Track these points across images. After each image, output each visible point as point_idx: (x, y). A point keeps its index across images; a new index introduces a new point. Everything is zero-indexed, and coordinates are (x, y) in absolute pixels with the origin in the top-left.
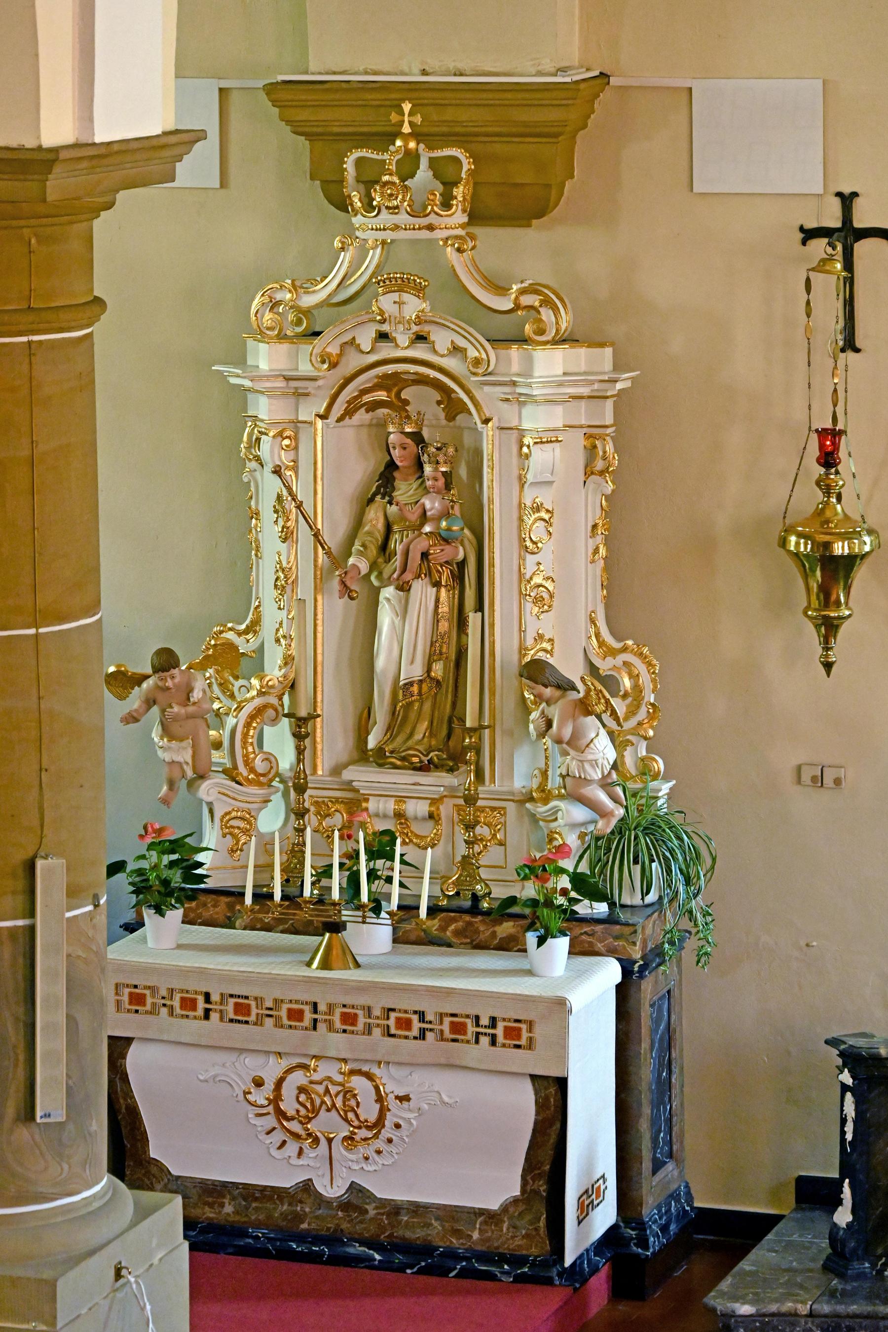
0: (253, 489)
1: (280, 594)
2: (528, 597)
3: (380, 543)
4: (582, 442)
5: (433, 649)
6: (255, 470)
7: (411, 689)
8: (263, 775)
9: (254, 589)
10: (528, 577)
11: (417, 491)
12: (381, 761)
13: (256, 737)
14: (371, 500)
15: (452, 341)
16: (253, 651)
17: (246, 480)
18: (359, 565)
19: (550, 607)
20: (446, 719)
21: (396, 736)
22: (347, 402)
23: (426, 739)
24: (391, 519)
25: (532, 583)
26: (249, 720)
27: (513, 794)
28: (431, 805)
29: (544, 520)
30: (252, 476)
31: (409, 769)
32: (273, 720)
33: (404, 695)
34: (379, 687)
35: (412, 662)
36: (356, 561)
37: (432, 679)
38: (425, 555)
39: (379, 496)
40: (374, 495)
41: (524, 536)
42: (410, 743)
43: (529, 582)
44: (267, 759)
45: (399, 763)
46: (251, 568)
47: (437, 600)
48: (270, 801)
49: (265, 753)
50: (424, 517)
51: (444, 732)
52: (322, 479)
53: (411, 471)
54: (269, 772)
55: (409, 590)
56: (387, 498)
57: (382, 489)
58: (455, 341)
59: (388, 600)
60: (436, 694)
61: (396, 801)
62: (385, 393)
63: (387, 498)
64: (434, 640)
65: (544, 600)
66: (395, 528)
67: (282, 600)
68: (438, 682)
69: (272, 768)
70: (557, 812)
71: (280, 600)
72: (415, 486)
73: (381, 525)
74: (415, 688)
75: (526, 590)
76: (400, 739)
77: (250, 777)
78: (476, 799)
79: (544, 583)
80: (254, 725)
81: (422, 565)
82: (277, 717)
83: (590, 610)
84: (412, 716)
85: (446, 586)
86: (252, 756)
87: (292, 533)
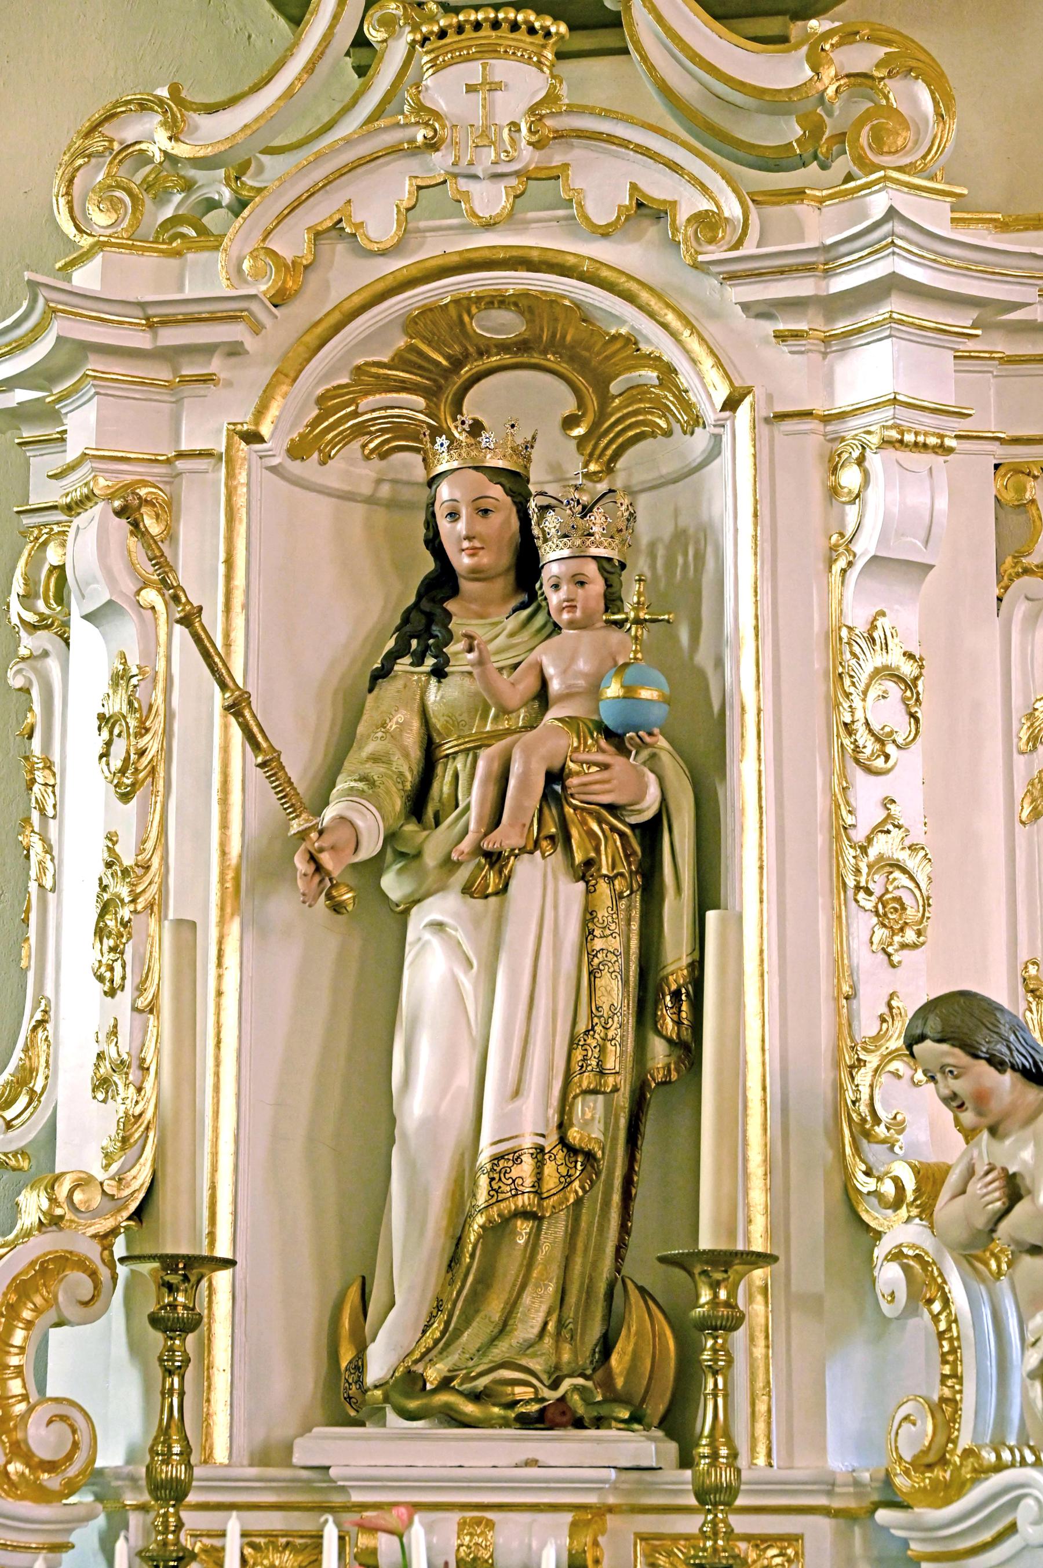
0: (37, 707)
1: (112, 950)
2: (861, 895)
3: (408, 786)
4: (990, 487)
5: (578, 1055)
6: (46, 654)
7: (515, 1172)
8: (51, 1467)
9: (31, 975)
10: (859, 835)
11: (516, 640)
12: (413, 1405)
13: (31, 1350)
14: (382, 674)
15: (634, 187)
16: (23, 1153)
17: (18, 682)
18: (360, 823)
19: (919, 933)
20: (602, 1288)
21: (458, 1333)
22: (321, 400)
23: (548, 1341)
24: (438, 723)
25: (873, 852)
26: (13, 1298)
27: (830, 1487)
28: (575, 1527)
29: (899, 679)
30: (35, 670)
31: (505, 1424)
32: (86, 1304)
33: (494, 1191)
34: (411, 1167)
35: (517, 1093)
36: (348, 808)
37: (572, 1150)
38: (555, 777)
39: (407, 660)
40: (393, 657)
41: (848, 719)
42: (501, 1350)
43: (864, 850)
44: (63, 1418)
45: (470, 1408)
46: (26, 921)
47: (589, 915)
48: (68, 1547)
49: (56, 1400)
50: (542, 697)
51: (596, 1331)
52: (246, 606)
53: (503, 585)
54: (69, 1457)
55: (503, 890)
56: (430, 662)
57: (414, 643)
58: (642, 185)
59: (438, 926)
60: (579, 1202)
61: (462, 1525)
62: (420, 402)
63: (430, 662)
64: (582, 1027)
65: (904, 908)
66: (448, 748)
67: (118, 966)
68: (589, 1156)
69: (75, 1445)
70: (1015, 1503)
71: (111, 969)
72: (512, 623)
73: (412, 740)
74: (526, 1168)
75: (857, 871)
76: (471, 1338)
77: (11, 1468)
78: (732, 1491)
79: (903, 856)
80: (27, 1314)
81: (546, 811)
82: (97, 1285)
83: (1024, 956)
84: (510, 1266)
85: (611, 879)
86: (20, 1408)
87: (153, 771)
